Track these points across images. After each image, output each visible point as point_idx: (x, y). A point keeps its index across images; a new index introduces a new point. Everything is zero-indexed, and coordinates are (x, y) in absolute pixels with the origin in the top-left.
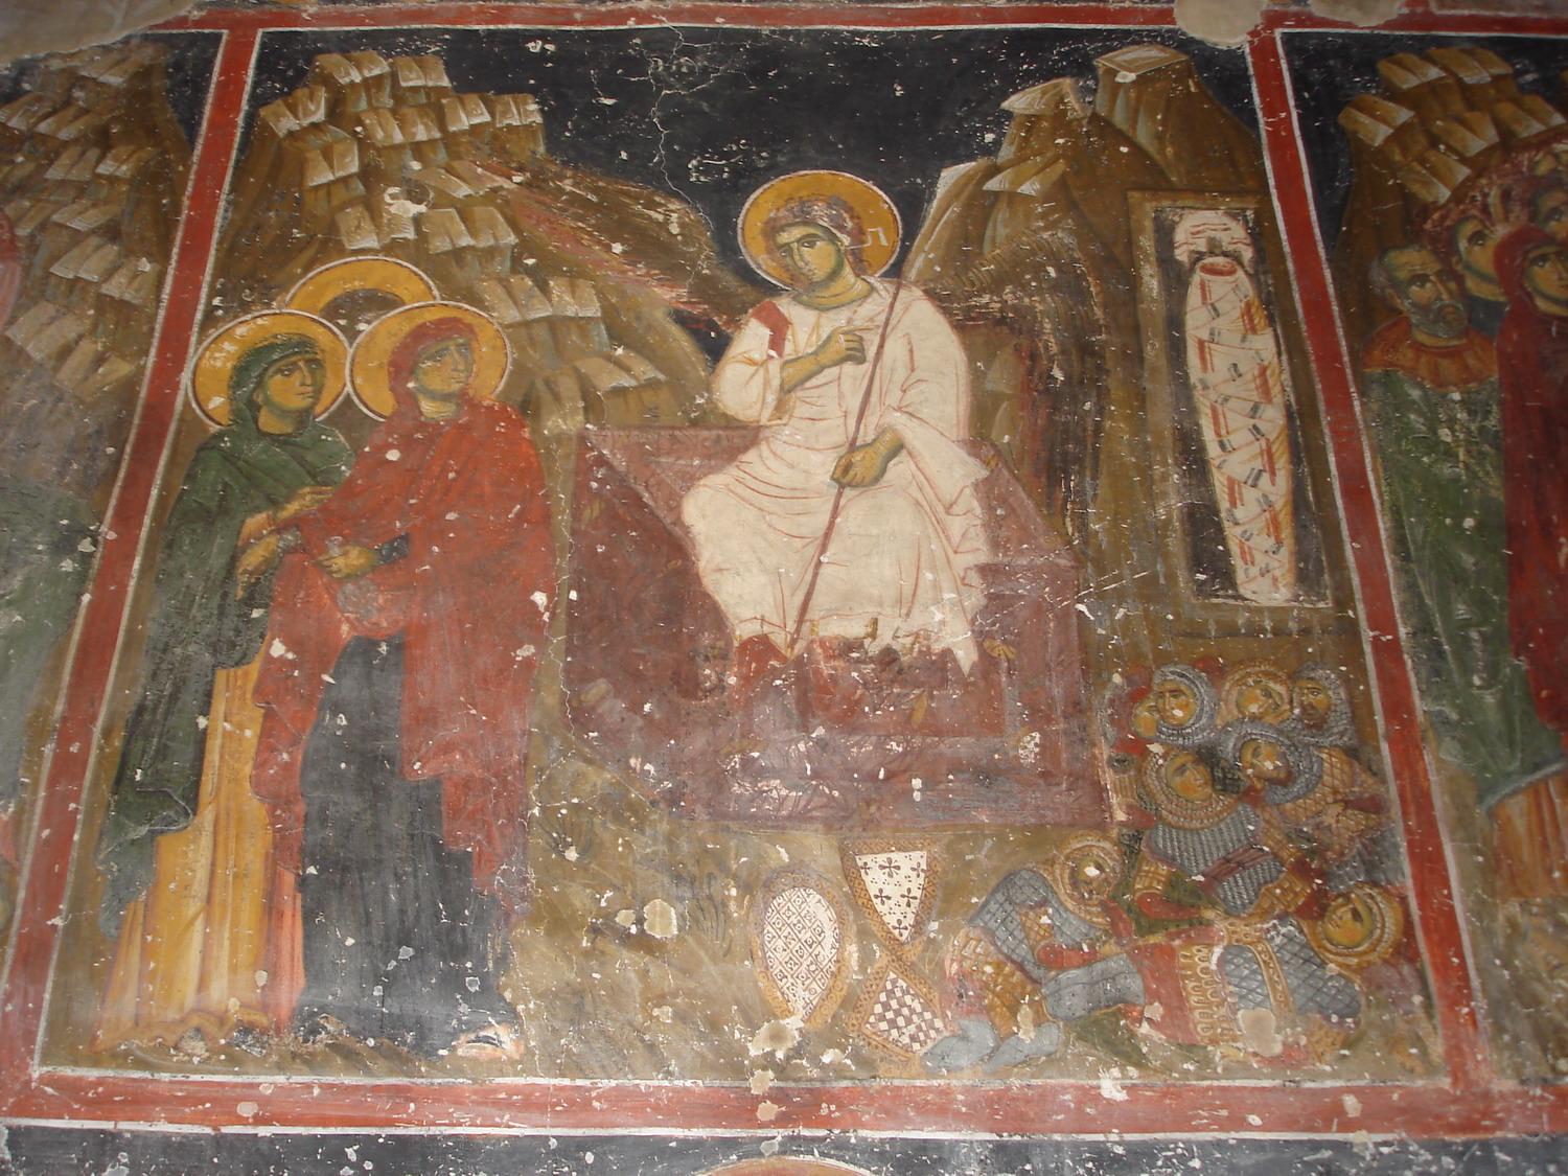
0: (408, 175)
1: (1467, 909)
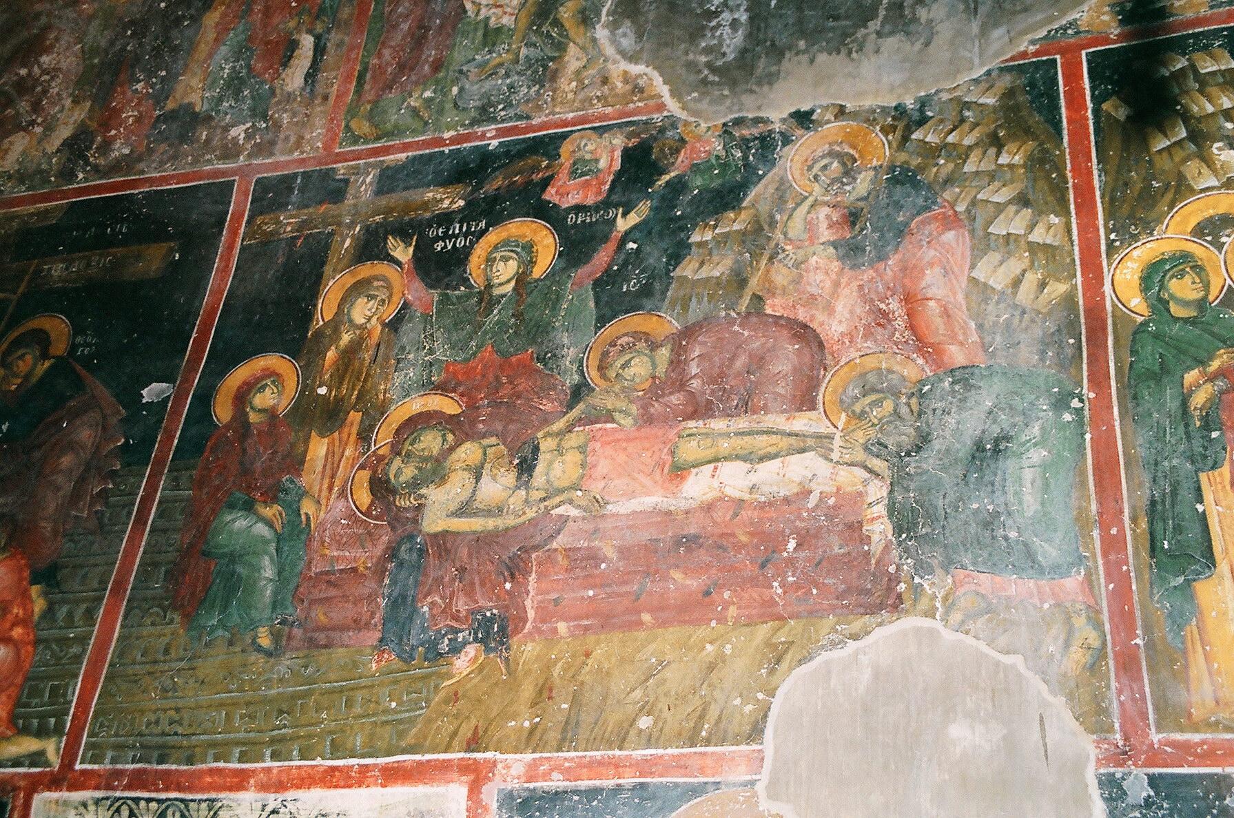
0: (1226, 133)
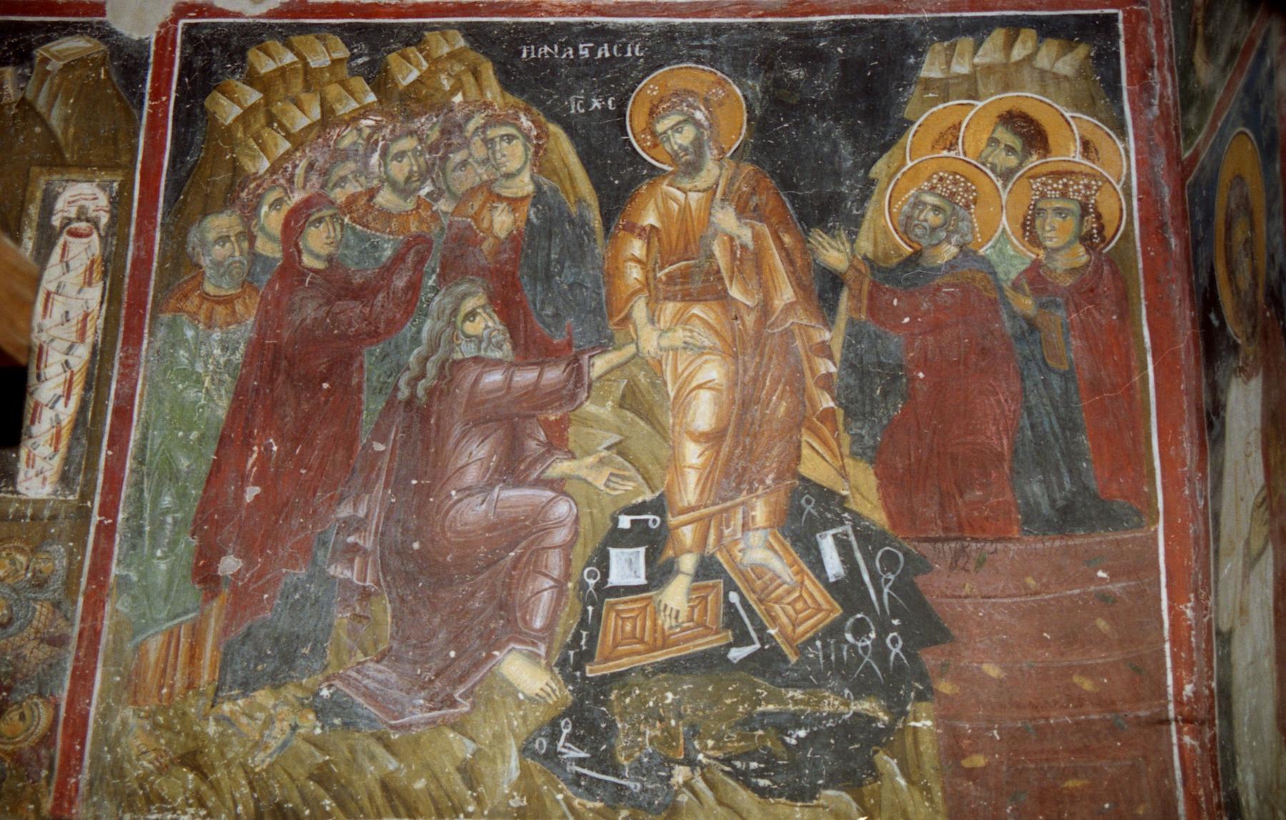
1: (98, 713)
